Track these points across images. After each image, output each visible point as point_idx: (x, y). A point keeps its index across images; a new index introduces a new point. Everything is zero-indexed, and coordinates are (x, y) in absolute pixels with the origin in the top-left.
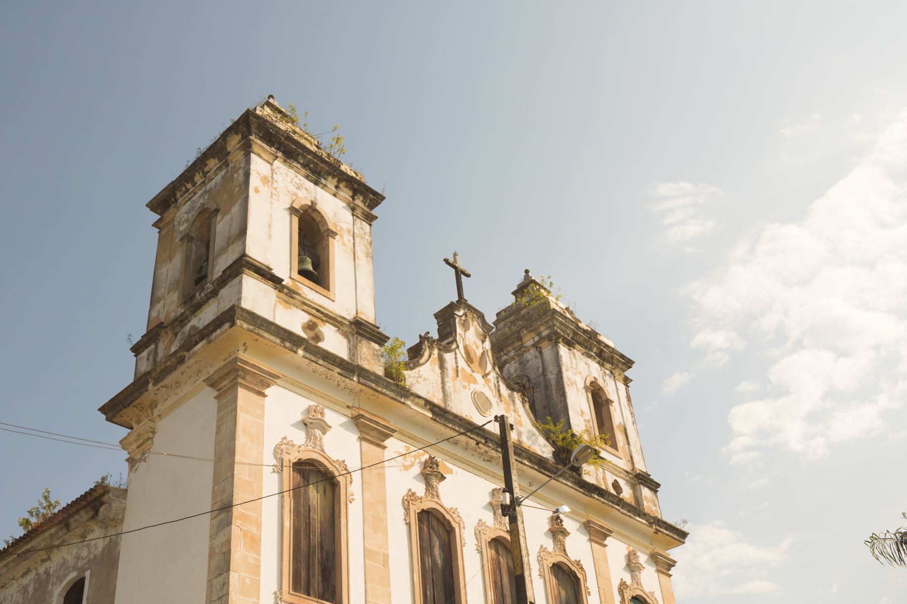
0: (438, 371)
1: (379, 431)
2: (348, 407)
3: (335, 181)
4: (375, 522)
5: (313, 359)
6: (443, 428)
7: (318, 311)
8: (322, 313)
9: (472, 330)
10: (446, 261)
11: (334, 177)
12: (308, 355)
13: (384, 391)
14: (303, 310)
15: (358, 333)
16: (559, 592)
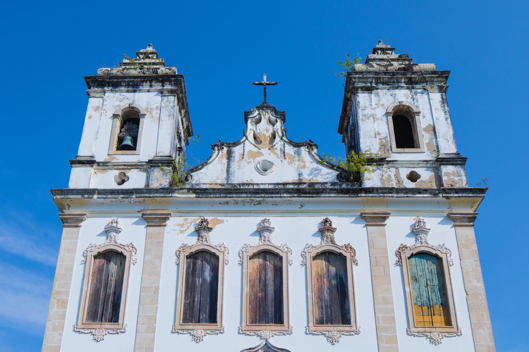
0: (225, 161)
2: (139, 212)
3: (148, 83)
4: (152, 270)
5: (104, 196)
6: (209, 199)
7: (125, 165)
8: (128, 165)
9: (264, 121)
11: (146, 82)
12: (100, 196)
13: (155, 195)
14: (115, 169)
15: (152, 166)
16: (328, 270)
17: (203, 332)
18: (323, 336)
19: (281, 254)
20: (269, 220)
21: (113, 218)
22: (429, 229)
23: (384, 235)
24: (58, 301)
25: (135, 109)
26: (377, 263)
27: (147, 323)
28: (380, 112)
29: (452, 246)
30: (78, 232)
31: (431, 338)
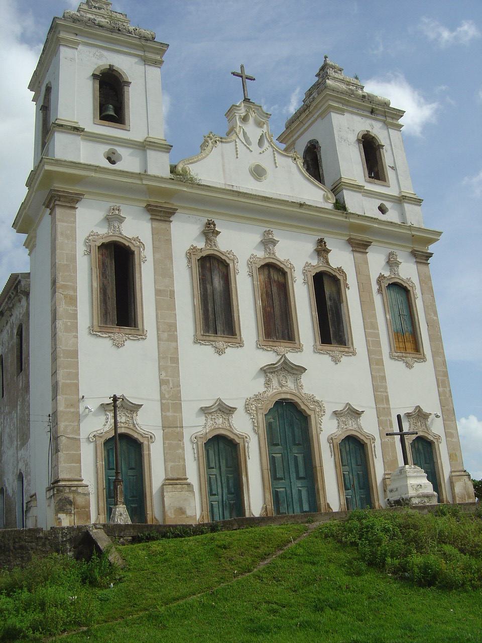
1: (164, 211)
4: (164, 271)
10: (234, 74)
17: (225, 345)
18: (328, 356)
19: (286, 270)
20: (272, 231)
21: (114, 204)
22: (401, 263)
23: (366, 263)
24: (66, 297)
25: (114, 73)
26: (364, 289)
27: (168, 331)
28: (353, 138)
29: (415, 280)
30: (75, 215)
31: (406, 363)
